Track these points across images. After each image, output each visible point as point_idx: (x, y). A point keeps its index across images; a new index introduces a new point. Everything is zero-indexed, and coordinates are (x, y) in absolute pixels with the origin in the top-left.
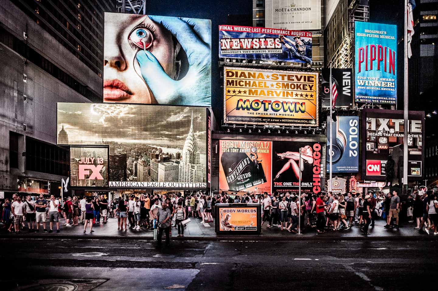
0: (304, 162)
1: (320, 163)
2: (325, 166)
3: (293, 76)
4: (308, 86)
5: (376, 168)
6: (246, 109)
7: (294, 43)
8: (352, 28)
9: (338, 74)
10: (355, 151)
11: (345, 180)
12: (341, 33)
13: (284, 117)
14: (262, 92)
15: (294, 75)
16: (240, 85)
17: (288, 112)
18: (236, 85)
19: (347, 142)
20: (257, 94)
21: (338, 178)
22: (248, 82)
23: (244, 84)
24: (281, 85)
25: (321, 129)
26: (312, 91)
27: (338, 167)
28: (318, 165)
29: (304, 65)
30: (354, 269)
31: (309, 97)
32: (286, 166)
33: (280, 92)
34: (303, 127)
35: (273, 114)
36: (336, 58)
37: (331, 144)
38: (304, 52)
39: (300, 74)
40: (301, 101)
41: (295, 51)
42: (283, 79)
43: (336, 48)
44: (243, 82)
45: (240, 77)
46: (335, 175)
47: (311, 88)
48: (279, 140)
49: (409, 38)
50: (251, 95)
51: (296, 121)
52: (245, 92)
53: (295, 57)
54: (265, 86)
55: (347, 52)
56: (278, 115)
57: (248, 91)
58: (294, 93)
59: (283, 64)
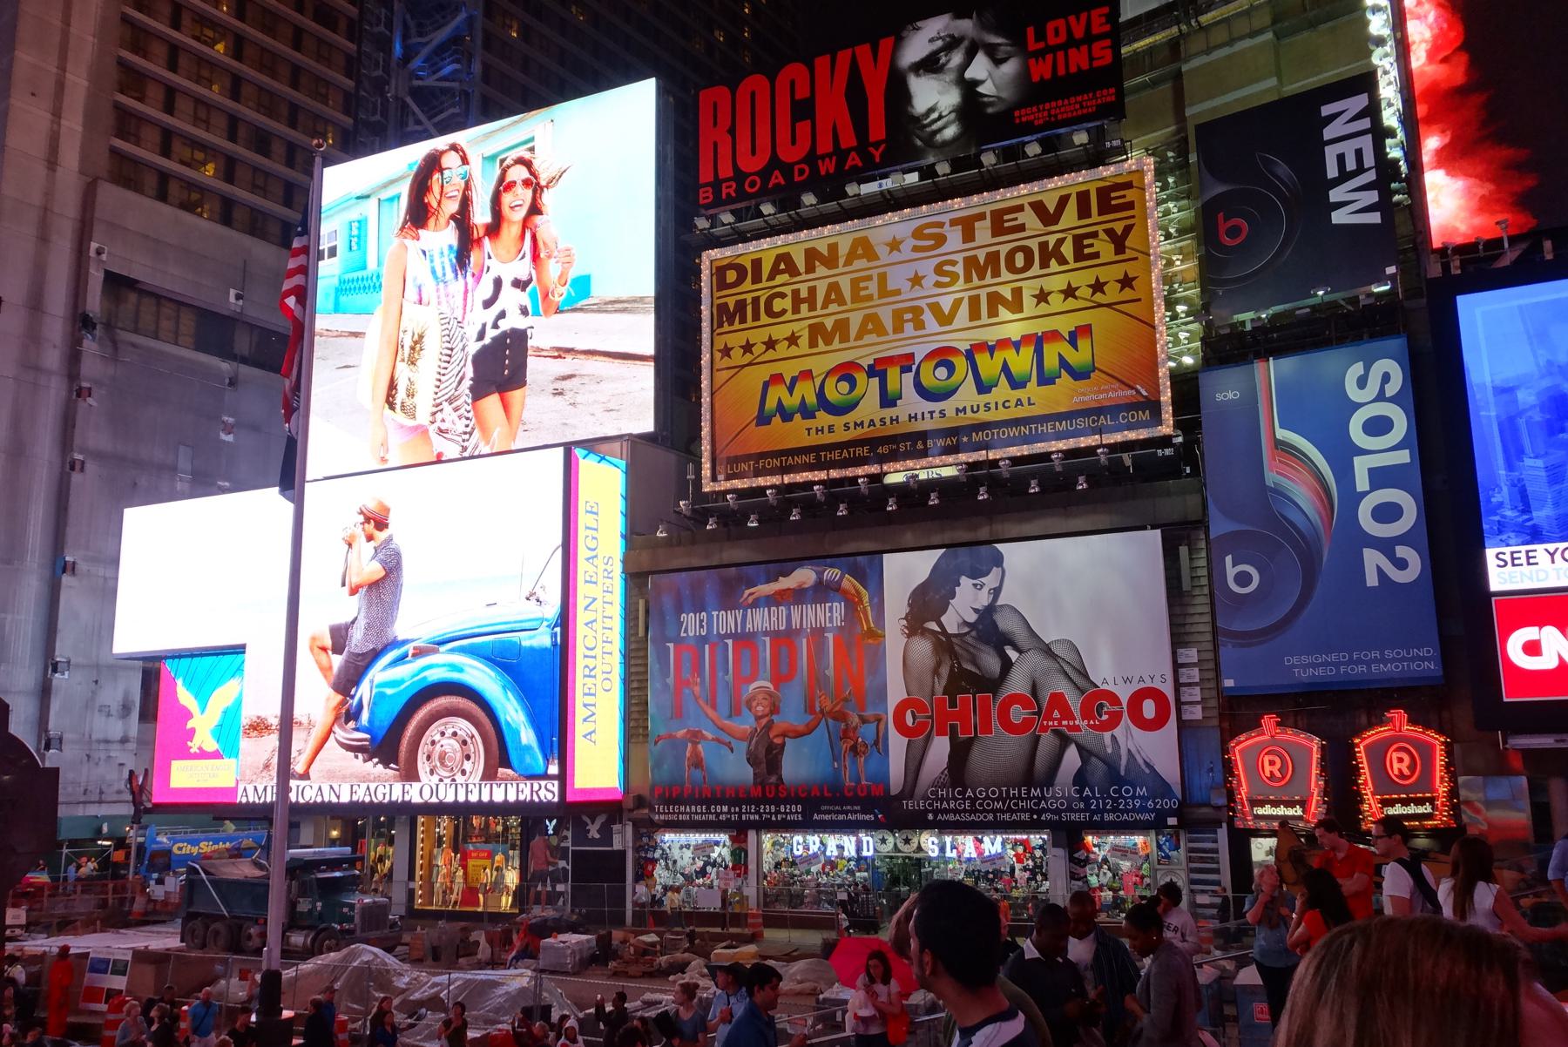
2: (1210, 656)
3: (1020, 208)
4: (1102, 235)
6: (798, 416)
10: (1402, 551)
13: (983, 416)
14: (872, 324)
15: (1025, 201)
16: (770, 312)
17: (1003, 391)
18: (756, 317)
20: (844, 339)
22: (804, 294)
23: (786, 303)
24: (959, 269)
26: (1129, 254)
27: (1295, 660)
31: (1112, 293)
33: (958, 303)
35: (927, 416)
40: (1065, 325)
42: (969, 235)
44: (783, 296)
45: (771, 277)
50: (822, 346)
52: (793, 340)
54: (884, 292)
56: (950, 413)
57: (806, 334)
58: (1029, 290)
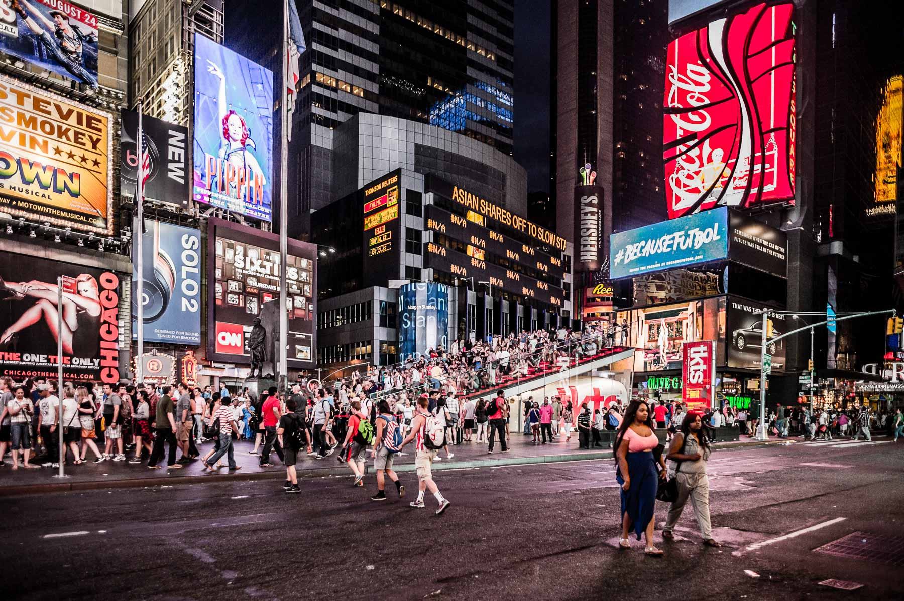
0: (78, 311)
1: (117, 318)
3: (49, 103)
5: (234, 340)
7: (51, 25)
8: (189, 45)
9: (157, 132)
11: (173, 358)
12: (167, 44)
13: (23, 195)
19: (177, 281)
21: (158, 354)
24: (15, 115)
25: (118, 243)
28: (112, 320)
29: (77, 85)
30: (185, 543)
31: (90, 164)
32: (31, 316)
34: (73, 229)
36: (154, 95)
37: (139, 278)
38: (78, 56)
39: (67, 104)
40: (70, 169)
41: (54, 45)
43: (154, 72)
46: (150, 345)
47: (95, 144)
48: (10, 249)
49: (290, 103)
51: (57, 212)
53: (55, 60)
55: (179, 90)
58: (52, 145)
59: (19, 65)
